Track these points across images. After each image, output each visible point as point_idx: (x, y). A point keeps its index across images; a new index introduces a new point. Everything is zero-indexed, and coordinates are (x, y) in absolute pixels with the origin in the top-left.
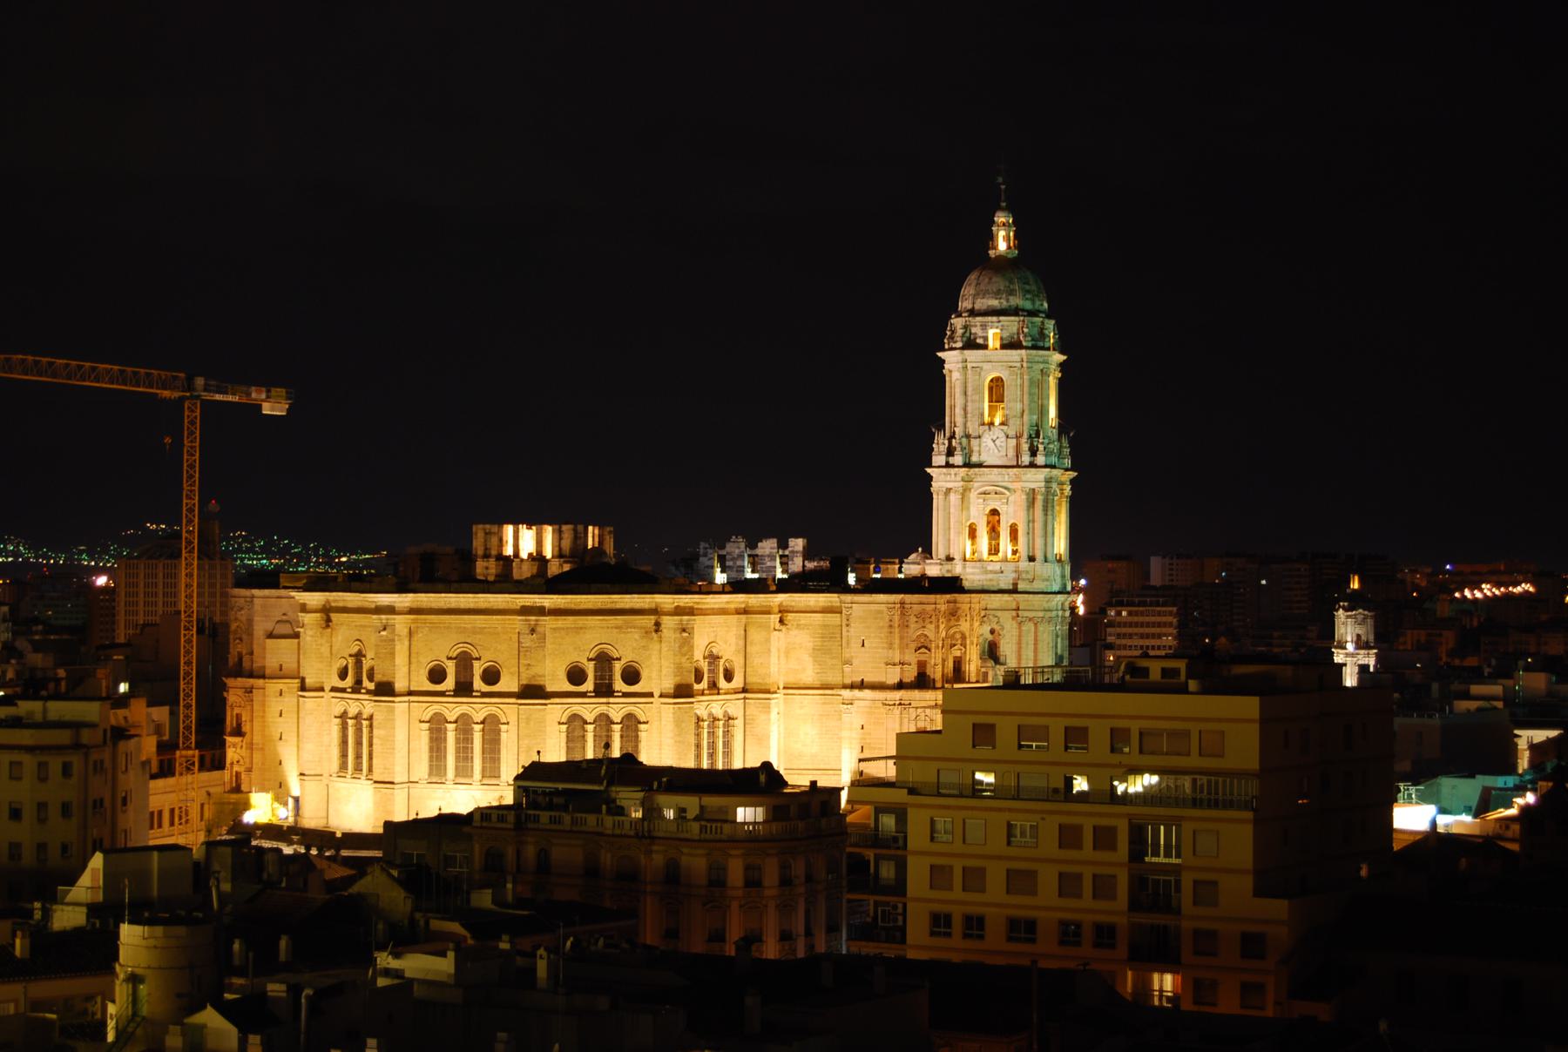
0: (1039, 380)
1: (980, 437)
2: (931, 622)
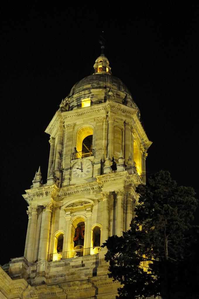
0: (122, 129)
1: (71, 168)
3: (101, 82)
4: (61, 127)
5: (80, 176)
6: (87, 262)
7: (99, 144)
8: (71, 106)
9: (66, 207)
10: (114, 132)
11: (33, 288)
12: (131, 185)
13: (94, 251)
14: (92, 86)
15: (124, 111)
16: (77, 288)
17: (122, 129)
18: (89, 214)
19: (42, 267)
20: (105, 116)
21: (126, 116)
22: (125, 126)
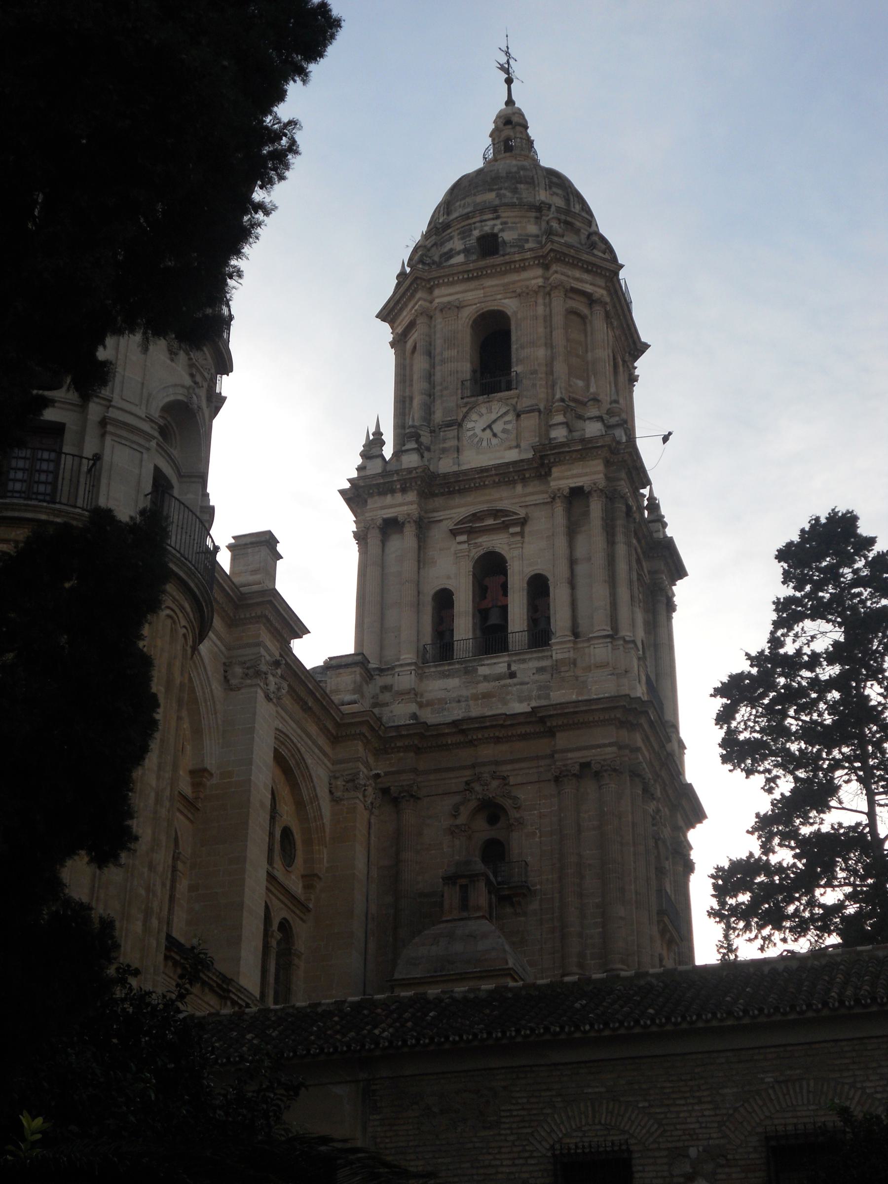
3: (522, 186)
5: (485, 443)
6: (522, 666)
9: (455, 525)
14: (498, 196)
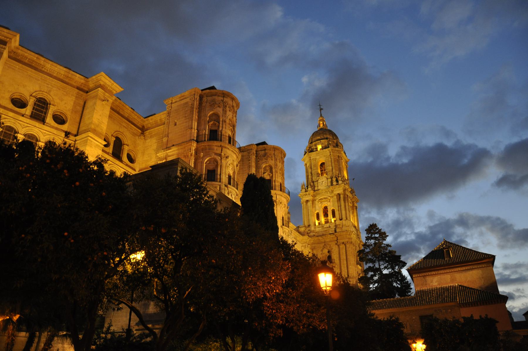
0: (337, 160)
1: (317, 181)
2: (219, 107)
4: (309, 160)
6: (332, 225)
7: (329, 168)
8: (312, 148)
10: (335, 161)
11: (311, 238)
12: (345, 189)
13: (333, 220)
15: (337, 151)
16: (329, 237)
17: (337, 160)
18: (329, 203)
19: (312, 228)
20: (329, 154)
21: (339, 153)
22: (338, 158)
